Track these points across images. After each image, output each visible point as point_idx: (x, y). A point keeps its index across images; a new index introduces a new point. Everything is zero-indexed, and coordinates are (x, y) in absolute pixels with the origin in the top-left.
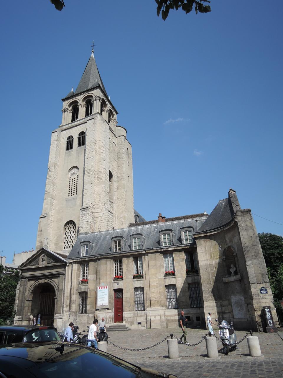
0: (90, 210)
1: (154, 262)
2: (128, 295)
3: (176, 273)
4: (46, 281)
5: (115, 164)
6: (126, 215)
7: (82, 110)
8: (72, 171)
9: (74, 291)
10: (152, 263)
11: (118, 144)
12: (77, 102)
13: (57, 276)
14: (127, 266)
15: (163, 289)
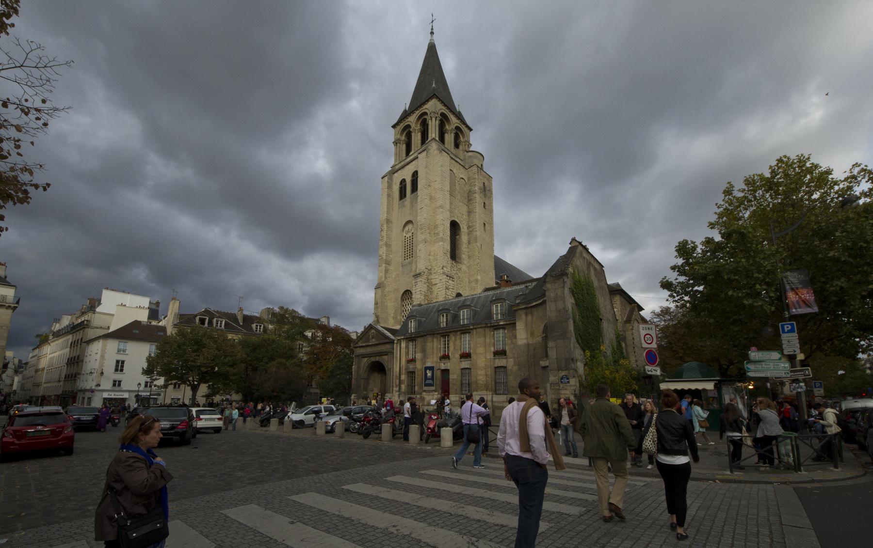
0: (425, 277)
1: (483, 339)
2: (454, 376)
3: (508, 353)
4: (377, 359)
5: (464, 209)
6: (479, 278)
7: (416, 138)
8: (407, 229)
9: (403, 371)
10: (481, 340)
11: (469, 179)
12: (409, 126)
13: (385, 353)
14: (454, 344)
15: (490, 372)
